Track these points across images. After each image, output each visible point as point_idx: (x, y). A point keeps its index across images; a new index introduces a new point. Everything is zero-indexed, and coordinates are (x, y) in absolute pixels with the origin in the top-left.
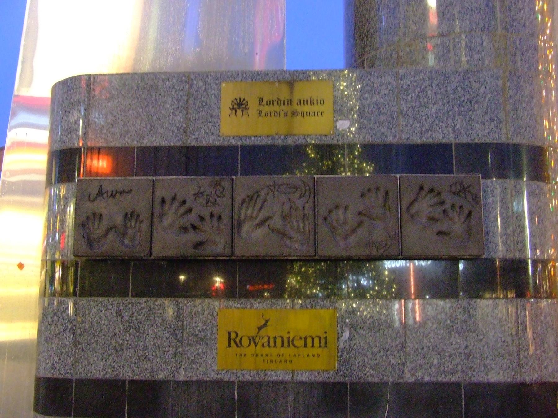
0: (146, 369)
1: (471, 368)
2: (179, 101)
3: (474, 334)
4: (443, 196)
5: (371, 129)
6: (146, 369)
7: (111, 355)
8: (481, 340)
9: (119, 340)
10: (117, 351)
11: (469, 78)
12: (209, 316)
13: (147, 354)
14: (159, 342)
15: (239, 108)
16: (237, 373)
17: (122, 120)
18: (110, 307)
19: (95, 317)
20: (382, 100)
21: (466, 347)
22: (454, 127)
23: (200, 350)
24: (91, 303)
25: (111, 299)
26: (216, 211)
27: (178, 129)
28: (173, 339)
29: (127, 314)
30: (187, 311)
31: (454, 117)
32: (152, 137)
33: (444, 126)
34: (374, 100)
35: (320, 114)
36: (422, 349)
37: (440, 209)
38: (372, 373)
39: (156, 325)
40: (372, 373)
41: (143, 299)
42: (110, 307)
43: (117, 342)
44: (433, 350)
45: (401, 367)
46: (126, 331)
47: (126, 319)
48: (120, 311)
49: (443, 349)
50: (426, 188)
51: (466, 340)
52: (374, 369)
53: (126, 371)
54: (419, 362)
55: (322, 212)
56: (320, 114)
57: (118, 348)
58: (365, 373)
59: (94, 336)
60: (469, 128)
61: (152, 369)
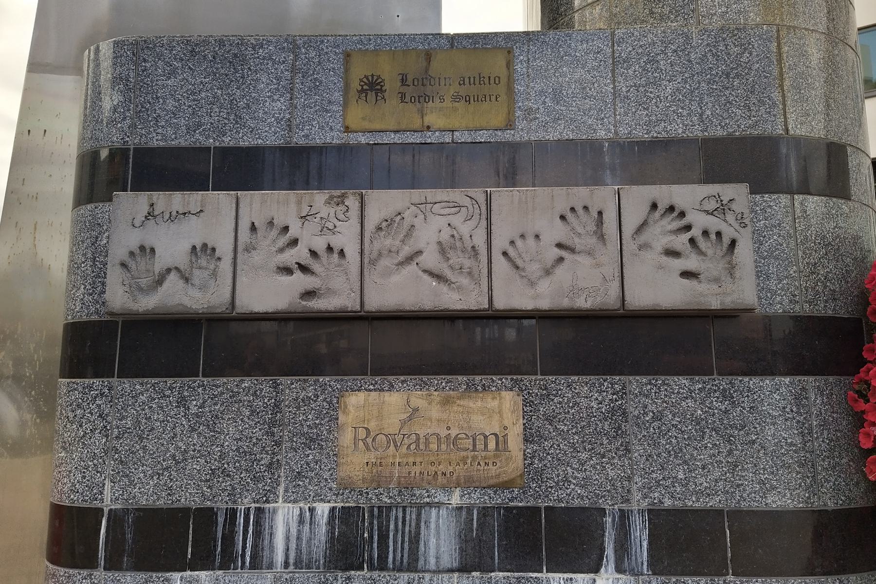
0: (224, 490)
1: (738, 486)
2: (279, 79)
3: (742, 432)
4: (689, 219)
5: (571, 119)
6: (224, 490)
7: (167, 468)
8: (754, 442)
9: (180, 444)
10: (177, 463)
11: (724, 39)
12: (325, 404)
13: (226, 466)
14: (244, 445)
15: (371, 90)
16: (367, 493)
17: (190, 106)
18: (168, 393)
19: (143, 410)
20: (589, 77)
21: (730, 452)
22: (701, 115)
23: (311, 457)
24: (138, 387)
25: (170, 381)
26: (337, 242)
27: (278, 121)
28: (267, 441)
29: (194, 403)
30: (288, 396)
31: (701, 99)
32: (238, 132)
33: (685, 113)
34: (577, 76)
35: (493, 98)
36: (659, 455)
37: (685, 237)
38: (579, 492)
39: (242, 420)
40: (579, 492)
41: (221, 379)
42: (168, 393)
43: (178, 448)
44: (676, 457)
45: (626, 483)
46: (193, 430)
47: (194, 410)
48: (183, 398)
49: (692, 455)
50: (662, 206)
51: (729, 441)
52: (582, 486)
53: (190, 493)
54: (654, 476)
55: (500, 242)
56: (493, 98)
57: (179, 457)
58: (568, 491)
59: (141, 438)
60: (725, 115)
61: (234, 489)
